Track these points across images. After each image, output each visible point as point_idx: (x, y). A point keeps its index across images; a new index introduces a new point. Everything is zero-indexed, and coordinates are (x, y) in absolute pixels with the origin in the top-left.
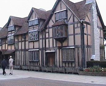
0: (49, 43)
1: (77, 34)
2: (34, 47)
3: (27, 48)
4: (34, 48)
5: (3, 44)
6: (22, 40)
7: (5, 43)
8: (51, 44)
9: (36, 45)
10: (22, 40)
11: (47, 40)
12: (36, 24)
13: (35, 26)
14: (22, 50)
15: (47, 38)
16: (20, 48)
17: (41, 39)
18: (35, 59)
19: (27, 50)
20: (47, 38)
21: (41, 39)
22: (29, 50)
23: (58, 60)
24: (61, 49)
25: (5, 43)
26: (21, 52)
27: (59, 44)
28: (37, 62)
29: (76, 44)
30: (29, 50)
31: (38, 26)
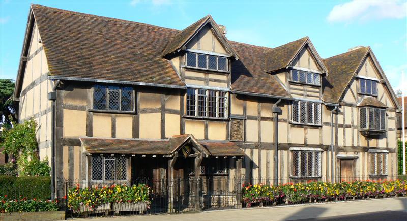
0: (345, 138)
1: (391, 129)
2: (305, 141)
3: (282, 140)
4: (306, 145)
5: (144, 111)
6: (259, 113)
7: (163, 111)
8: (351, 138)
9: (313, 137)
10: (259, 113)
11: (340, 130)
12: (313, 84)
13: (308, 88)
14: (260, 146)
15: (341, 126)
16: (252, 137)
17: (326, 124)
18: (303, 173)
19: (285, 147)
20: (341, 126)
21: (326, 124)
22: (292, 149)
23: (361, 174)
24: (367, 151)
25: (159, 106)
26: (256, 151)
27: (362, 142)
28: (317, 179)
29: (389, 147)
30: (292, 149)
31: (318, 90)
